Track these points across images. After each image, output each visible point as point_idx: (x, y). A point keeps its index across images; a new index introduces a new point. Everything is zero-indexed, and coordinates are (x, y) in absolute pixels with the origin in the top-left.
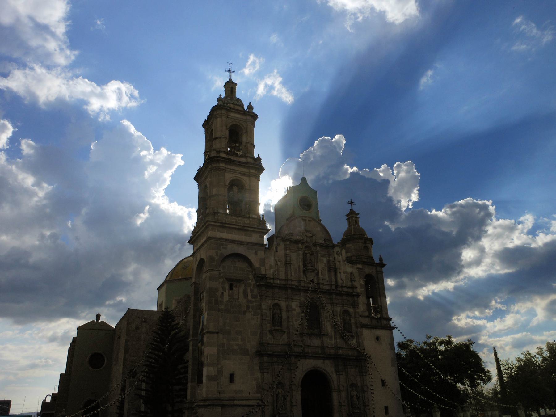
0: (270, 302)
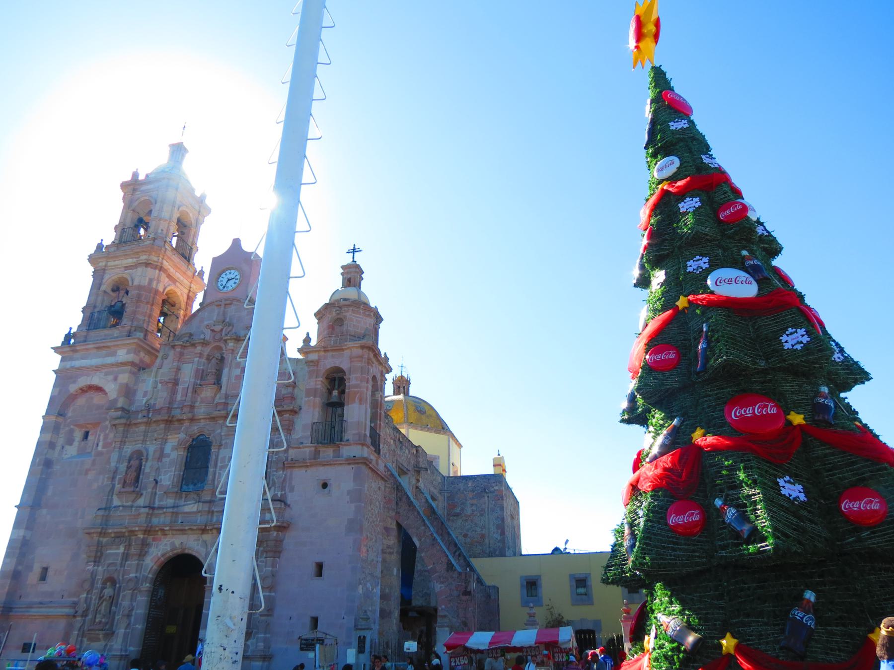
0: (129, 449)
